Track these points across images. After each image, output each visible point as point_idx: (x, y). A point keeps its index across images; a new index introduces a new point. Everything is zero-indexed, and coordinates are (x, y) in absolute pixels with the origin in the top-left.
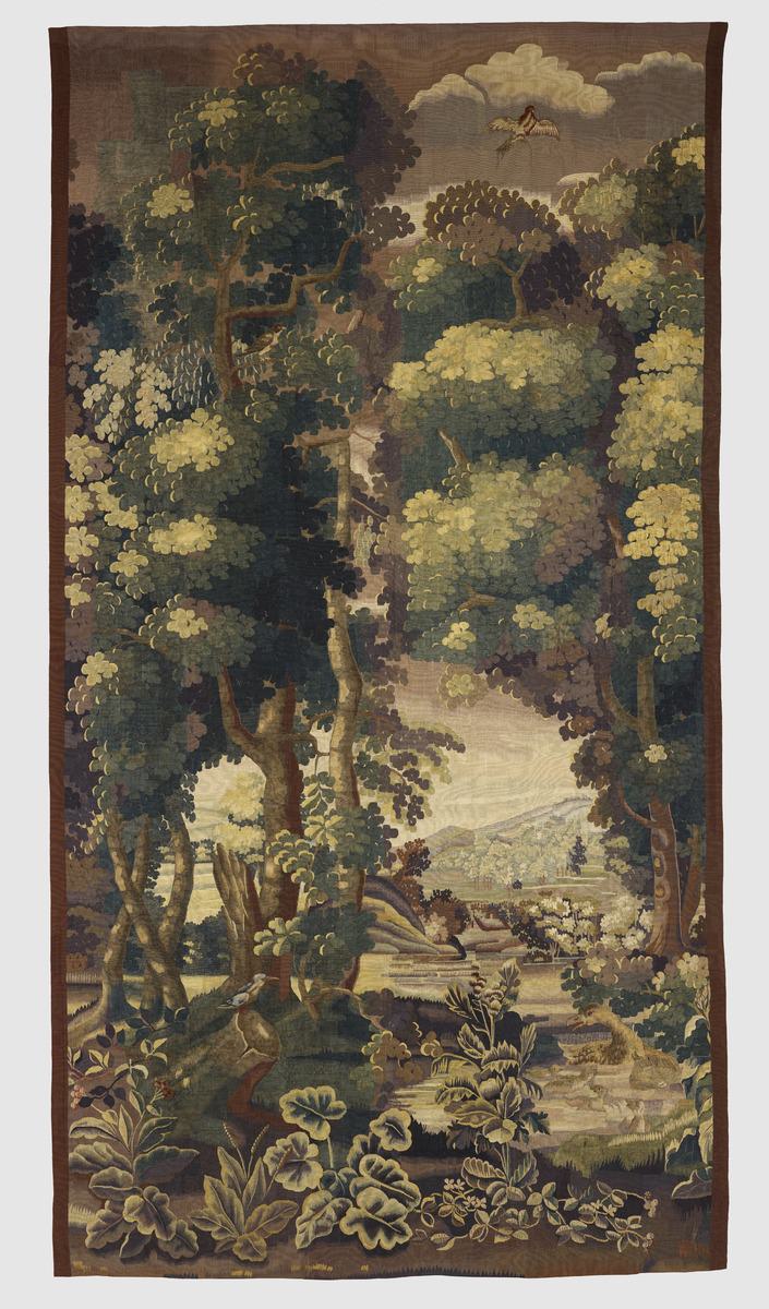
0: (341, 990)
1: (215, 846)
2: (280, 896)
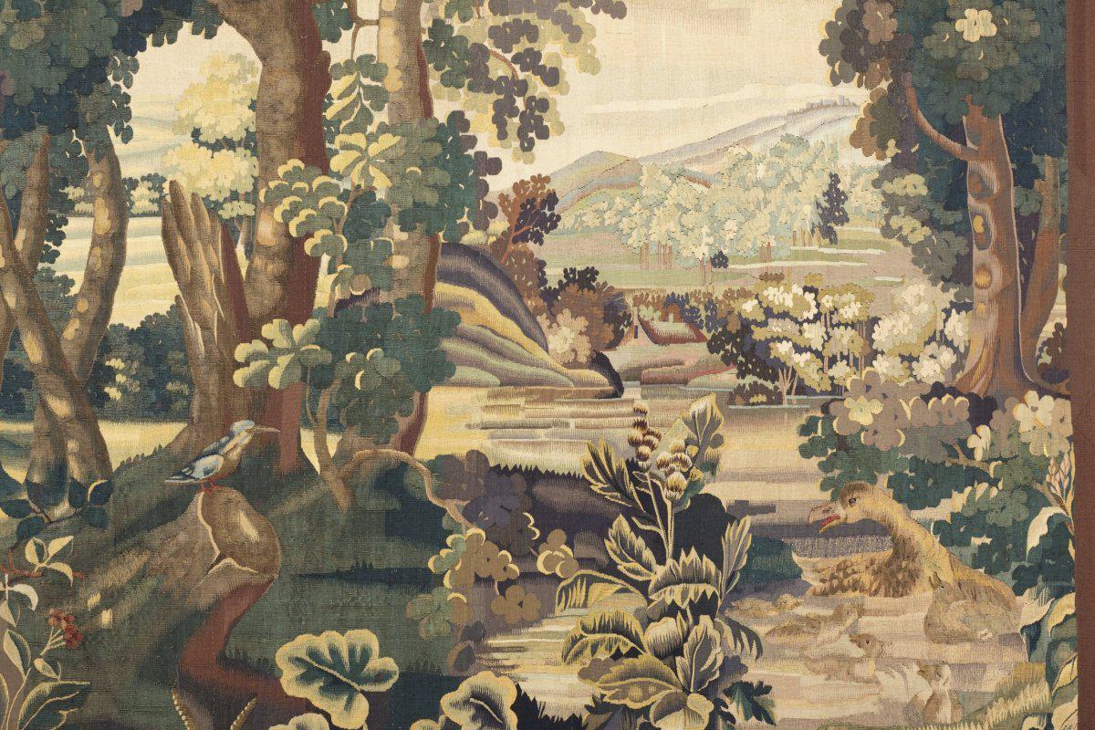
0: (391, 452)
1: (166, 186)
2: (280, 279)
